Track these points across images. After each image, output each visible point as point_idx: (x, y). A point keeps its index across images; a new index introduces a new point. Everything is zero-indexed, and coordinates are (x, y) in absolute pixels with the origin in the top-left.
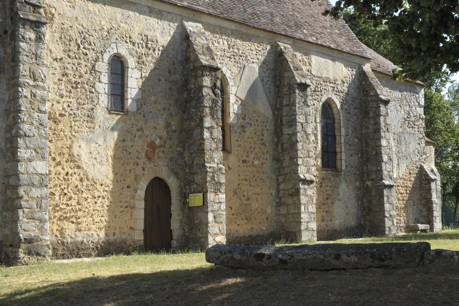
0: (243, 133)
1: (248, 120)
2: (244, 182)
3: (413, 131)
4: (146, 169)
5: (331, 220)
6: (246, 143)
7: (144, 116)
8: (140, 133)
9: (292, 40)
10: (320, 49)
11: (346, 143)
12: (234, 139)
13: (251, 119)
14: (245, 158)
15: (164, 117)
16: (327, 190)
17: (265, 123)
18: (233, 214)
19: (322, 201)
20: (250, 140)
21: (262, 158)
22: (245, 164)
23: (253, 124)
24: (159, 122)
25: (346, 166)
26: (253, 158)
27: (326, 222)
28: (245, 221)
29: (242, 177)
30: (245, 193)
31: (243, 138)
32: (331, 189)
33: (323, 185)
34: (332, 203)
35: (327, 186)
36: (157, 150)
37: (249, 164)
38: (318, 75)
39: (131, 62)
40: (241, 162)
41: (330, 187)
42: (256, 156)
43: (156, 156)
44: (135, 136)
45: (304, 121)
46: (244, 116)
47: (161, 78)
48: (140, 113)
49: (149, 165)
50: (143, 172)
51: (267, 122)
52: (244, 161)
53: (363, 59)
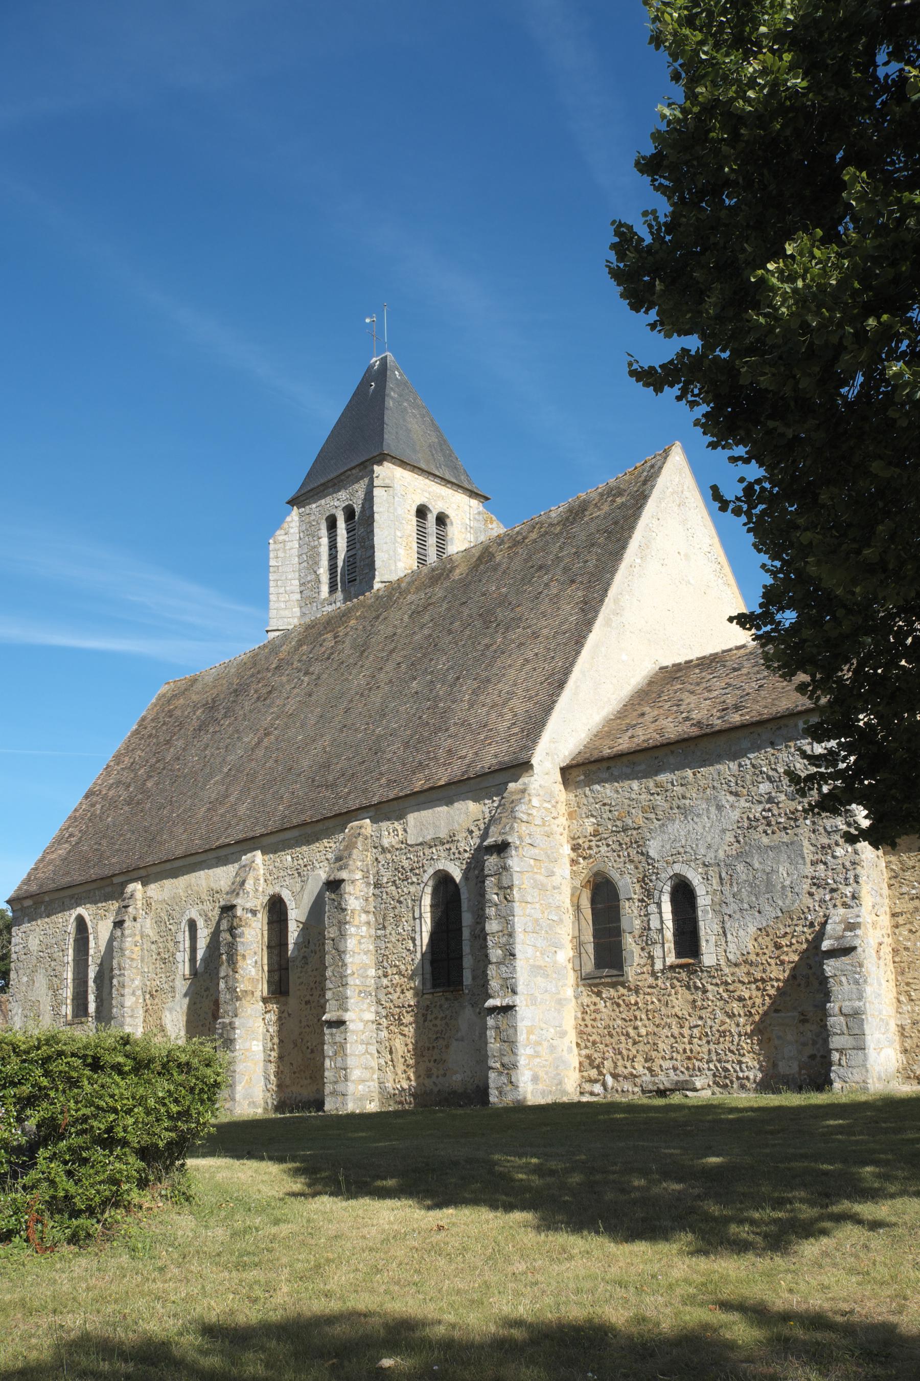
2: (307, 1030)
3: (786, 839)
5: (445, 1075)
9: (372, 808)
10: (422, 798)
12: (294, 977)
16: (436, 1025)
18: (294, 1073)
19: (427, 1045)
22: (308, 1006)
25: (474, 978)
27: (434, 1079)
28: (309, 1081)
30: (309, 1044)
31: (306, 972)
32: (444, 1022)
33: (429, 1017)
34: (447, 1047)
35: (436, 1018)
38: (418, 842)
40: (303, 1003)
41: (442, 1019)
45: (338, 933)
52: (307, 1003)
53: (512, 770)
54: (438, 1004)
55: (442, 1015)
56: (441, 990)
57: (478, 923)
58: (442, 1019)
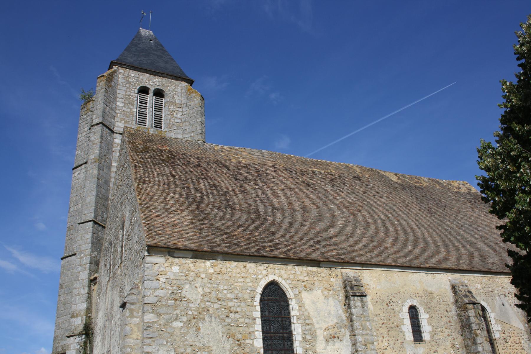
1: (507, 334)
20: (512, 347)
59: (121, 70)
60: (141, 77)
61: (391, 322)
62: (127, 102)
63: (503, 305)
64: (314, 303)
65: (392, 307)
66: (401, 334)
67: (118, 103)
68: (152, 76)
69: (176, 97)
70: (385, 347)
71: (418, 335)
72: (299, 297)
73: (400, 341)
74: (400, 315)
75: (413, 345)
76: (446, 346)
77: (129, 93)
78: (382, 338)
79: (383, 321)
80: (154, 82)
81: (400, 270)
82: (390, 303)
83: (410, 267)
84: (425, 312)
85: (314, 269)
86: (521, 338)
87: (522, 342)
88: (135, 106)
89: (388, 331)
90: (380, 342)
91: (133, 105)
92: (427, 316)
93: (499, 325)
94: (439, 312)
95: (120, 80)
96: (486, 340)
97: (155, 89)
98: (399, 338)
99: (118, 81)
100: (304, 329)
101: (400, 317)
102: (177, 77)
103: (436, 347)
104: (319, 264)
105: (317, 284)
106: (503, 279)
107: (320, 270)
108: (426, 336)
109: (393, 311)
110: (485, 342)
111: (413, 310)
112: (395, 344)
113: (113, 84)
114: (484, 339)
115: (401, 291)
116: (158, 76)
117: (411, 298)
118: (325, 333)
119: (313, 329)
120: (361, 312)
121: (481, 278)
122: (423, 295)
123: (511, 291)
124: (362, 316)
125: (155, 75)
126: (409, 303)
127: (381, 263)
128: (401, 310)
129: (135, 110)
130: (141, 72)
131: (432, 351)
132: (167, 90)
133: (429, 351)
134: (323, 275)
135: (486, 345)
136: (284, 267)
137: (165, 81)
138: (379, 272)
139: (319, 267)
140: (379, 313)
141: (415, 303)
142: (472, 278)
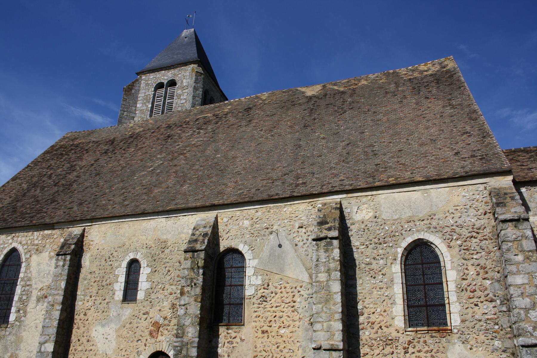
0: (265, 303)
4: (148, 345)
6: (269, 313)
7: (151, 302)
8: (146, 316)
11: (461, 290)
13: (276, 288)
14: (265, 328)
15: (170, 300)
17: (298, 288)
20: (274, 309)
21: (292, 326)
22: (266, 335)
23: (278, 291)
24: (164, 304)
25: (463, 321)
26: (277, 327)
29: (258, 349)
33: (411, 350)
35: (419, 351)
36: (161, 329)
37: (273, 334)
39: (144, 263)
40: (260, 332)
41: (427, 352)
42: (282, 325)
43: (160, 333)
44: (140, 319)
46: (266, 286)
47: (170, 269)
48: (147, 300)
49: (151, 340)
50: (145, 348)
51: (301, 287)
54: (422, 340)
55: (427, 348)
56: (425, 328)
57: (464, 279)
58: (427, 352)
59: (143, 77)
60: (158, 76)
61: (104, 279)
62: (145, 101)
63: (280, 246)
64: (39, 264)
65: (110, 263)
66: (111, 292)
67: (138, 105)
68: (166, 72)
69: (184, 81)
70: (89, 307)
71: (130, 293)
72: (29, 260)
73: (107, 300)
74: (117, 271)
75: (120, 305)
76: (163, 307)
77: (147, 93)
78: (89, 298)
79: (95, 279)
80: (164, 77)
81: (133, 219)
82: (109, 258)
83: (144, 214)
84: (148, 266)
85: (47, 232)
86: (297, 295)
87: (298, 300)
88: (151, 103)
89: (99, 290)
90: (85, 302)
91: (149, 102)
92: (148, 270)
93: (260, 277)
94: (168, 265)
95: (142, 86)
96: (195, 300)
97: (168, 81)
98: (107, 297)
99: (140, 87)
100: (23, 290)
101: (116, 273)
102: (185, 63)
103: (148, 308)
104: (54, 226)
105: (47, 246)
106: (297, 206)
107: (54, 232)
108: (140, 295)
109: (111, 267)
110: (193, 303)
111: (133, 266)
112: (100, 303)
113: (133, 91)
114: (192, 299)
115: (127, 243)
116: (171, 69)
117: (136, 251)
118: (39, 293)
119: (30, 290)
120: (60, 272)
121: (254, 211)
122: (153, 246)
123: (305, 223)
124: (60, 275)
125: (169, 69)
126: (132, 256)
127: (118, 215)
128: (120, 266)
129: (150, 106)
130: (158, 71)
131: (142, 312)
132: (177, 79)
133: (137, 312)
134: (55, 236)
135: (193, 306)
136: (26, 234)
137: (176, 71)
138: (109, 225)
139: (54, 229)
140: (94, 270)
141: (139, 257)
142: (238, 213)
